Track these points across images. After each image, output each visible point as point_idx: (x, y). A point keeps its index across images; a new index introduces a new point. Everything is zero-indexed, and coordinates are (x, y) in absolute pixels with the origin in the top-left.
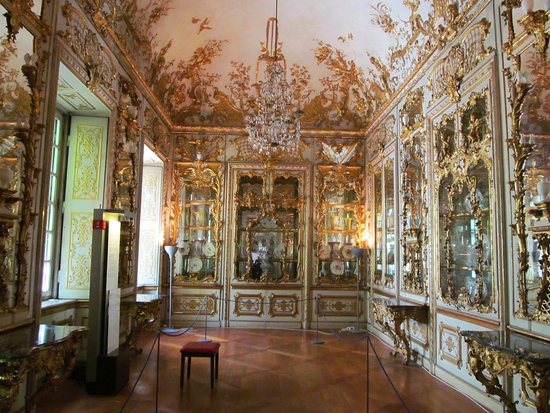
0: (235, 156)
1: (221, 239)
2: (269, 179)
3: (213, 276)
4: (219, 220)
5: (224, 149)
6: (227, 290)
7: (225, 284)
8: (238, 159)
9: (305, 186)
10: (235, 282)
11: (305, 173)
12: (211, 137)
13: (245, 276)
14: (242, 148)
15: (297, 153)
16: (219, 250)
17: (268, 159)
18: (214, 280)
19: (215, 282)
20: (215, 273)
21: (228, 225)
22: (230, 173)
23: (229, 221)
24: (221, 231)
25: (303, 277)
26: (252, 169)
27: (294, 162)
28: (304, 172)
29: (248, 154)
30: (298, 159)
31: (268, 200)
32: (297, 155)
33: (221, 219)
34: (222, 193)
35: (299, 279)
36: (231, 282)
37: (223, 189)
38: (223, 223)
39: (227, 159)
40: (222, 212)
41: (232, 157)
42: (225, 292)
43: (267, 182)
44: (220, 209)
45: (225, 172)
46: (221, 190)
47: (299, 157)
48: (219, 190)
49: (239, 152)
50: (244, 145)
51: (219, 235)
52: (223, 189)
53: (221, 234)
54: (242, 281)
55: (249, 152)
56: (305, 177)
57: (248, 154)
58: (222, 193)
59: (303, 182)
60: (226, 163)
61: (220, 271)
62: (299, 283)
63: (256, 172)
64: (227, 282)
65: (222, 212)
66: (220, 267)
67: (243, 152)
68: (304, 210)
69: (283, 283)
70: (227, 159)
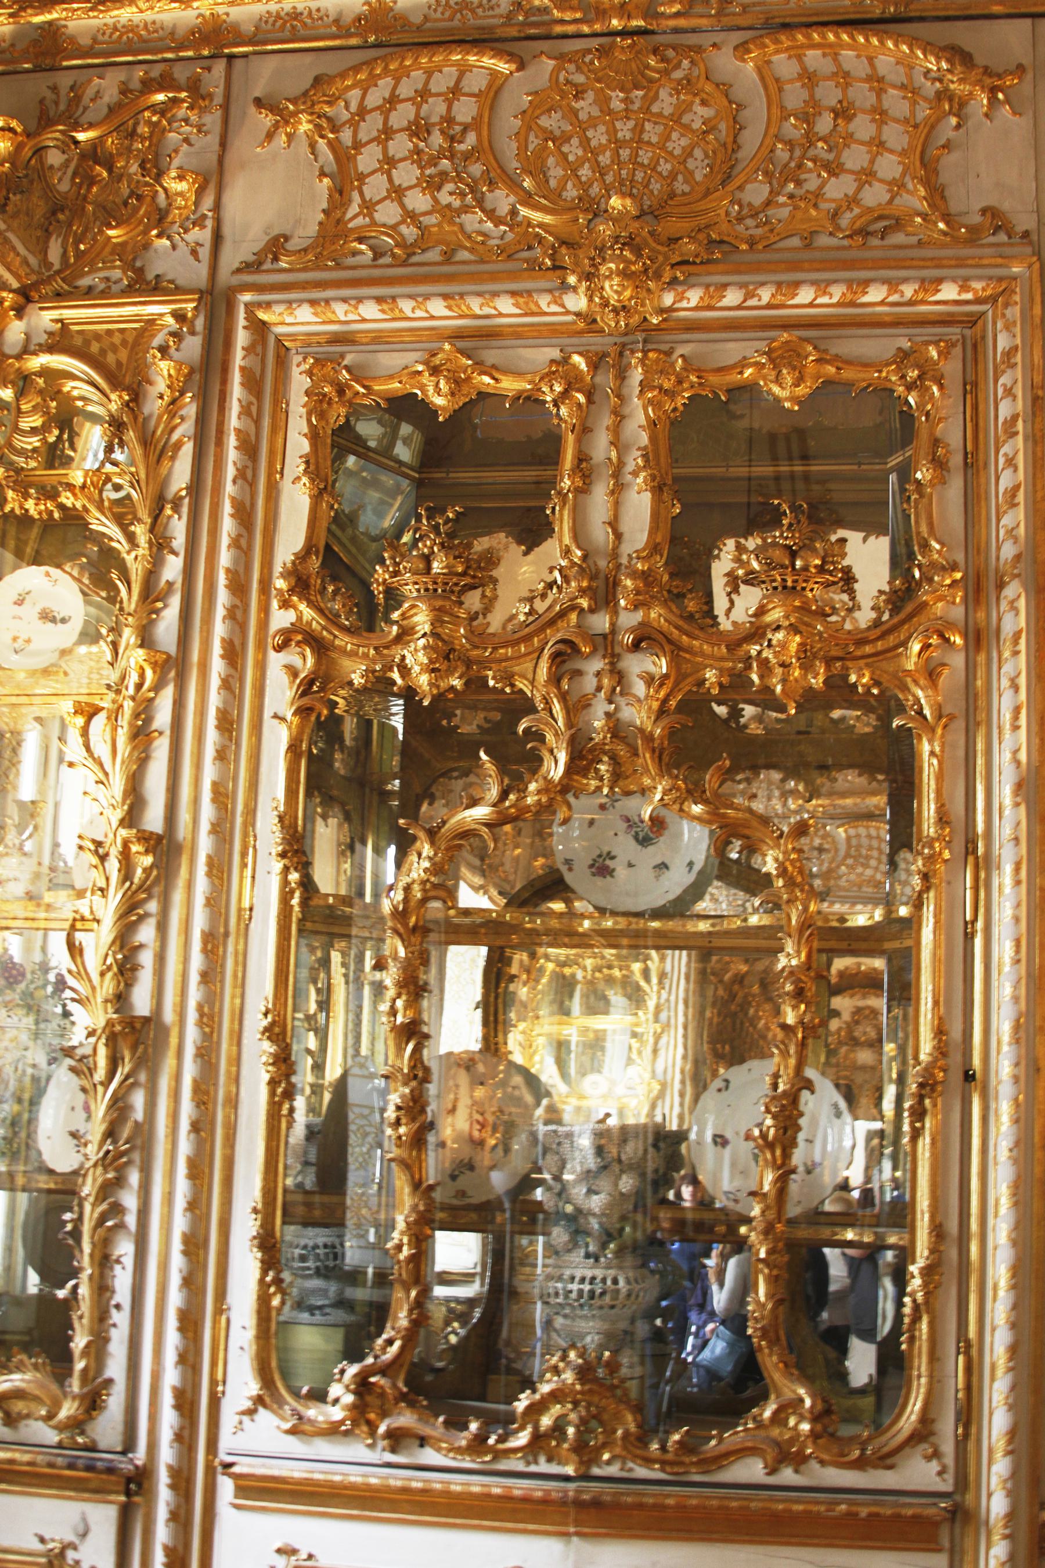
0: (308, 227)
1: (141, 1003)
2: (620, 417)
3: (60, 1360)
4: (132, 818)
5: (213, 179)
6: (180, 1518)
7: (167, 1455)
8: (328, 257)
9: (974, 464)
10: (256, 1439)
11: (975, 350)
12: (107, 87)
13: (362, 1386)
14: (367, 160)
15: (889, 166)
16: (119, 1107)
17: (605, 229)
18: (67, 1410)
19: (77, 1425)
20: (80, 1342)
21: (219, 869)
22: (253, 383)
23: (221, 830)
24: (146, 933)
25: (969, 1414)
26: (456, 336)
27: (870, 242)
28: (967, 329)
29: (418, 201)
30: (898, 224)
31: (601, 622)
32: (897, 186)
33: (154, 820)
34: (173, 568)
35: (924, 1433)
36: (227, 1441)
37: (178, 529)
38: (166, 847)
39: (231, 258)
40: (161, 749)
41: (276, 246)
42: (162, 1533)
43: (601, 447)
44: (144, 711)
45: (206, 377)
46: (160, 545)
47: (915, 198)
48: (140, 531)
49: (340, 194)
50: (387, 132)
51: (126, 970)
52: (178, 529)
53: (146, 959)
54: (333, 1431)
55: (432, 185)
56: (972, 388)
57: (418, 201)
58: (173, 568)
59: (952, 433)
60: (216, 302)
61: (121, 1319)
62: (920, 1473)
63: (491, 356)
64: (185, 1439)
65: (161, 749)
66: (122, 1280)
67: (376, 186)
68: (972, 712)
69: (752, 1470)
70: (231, 258)
